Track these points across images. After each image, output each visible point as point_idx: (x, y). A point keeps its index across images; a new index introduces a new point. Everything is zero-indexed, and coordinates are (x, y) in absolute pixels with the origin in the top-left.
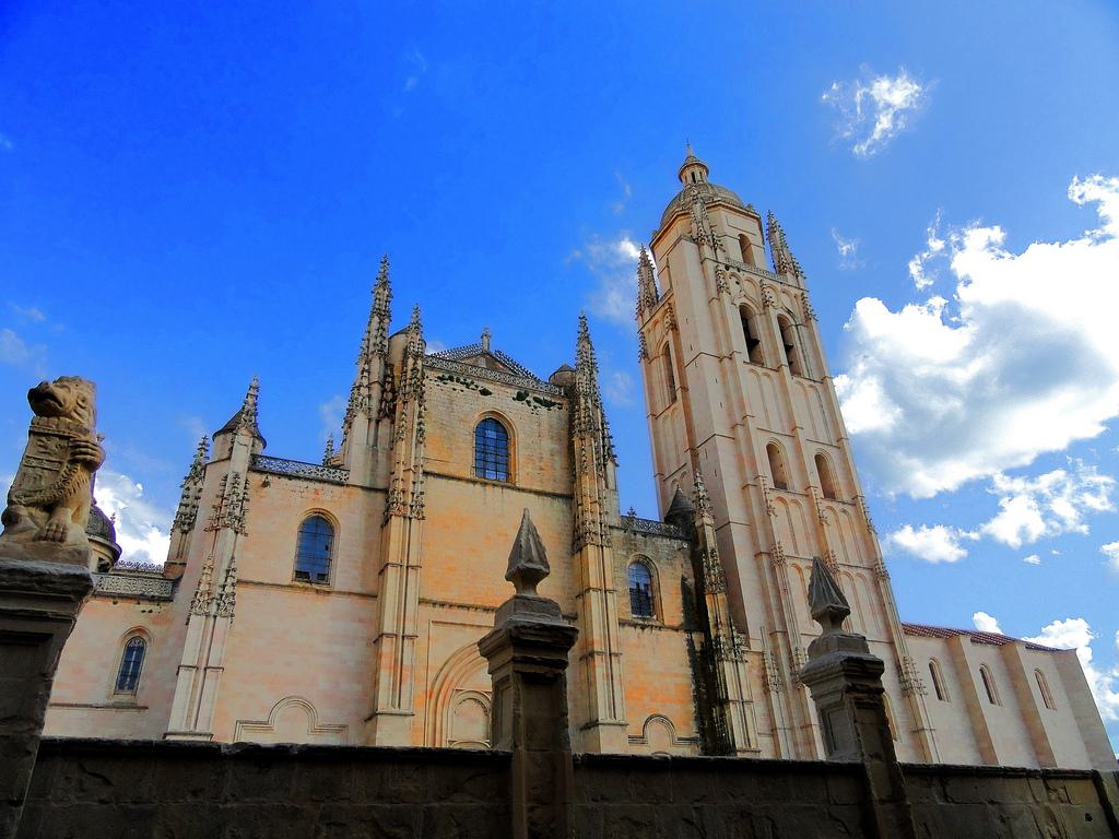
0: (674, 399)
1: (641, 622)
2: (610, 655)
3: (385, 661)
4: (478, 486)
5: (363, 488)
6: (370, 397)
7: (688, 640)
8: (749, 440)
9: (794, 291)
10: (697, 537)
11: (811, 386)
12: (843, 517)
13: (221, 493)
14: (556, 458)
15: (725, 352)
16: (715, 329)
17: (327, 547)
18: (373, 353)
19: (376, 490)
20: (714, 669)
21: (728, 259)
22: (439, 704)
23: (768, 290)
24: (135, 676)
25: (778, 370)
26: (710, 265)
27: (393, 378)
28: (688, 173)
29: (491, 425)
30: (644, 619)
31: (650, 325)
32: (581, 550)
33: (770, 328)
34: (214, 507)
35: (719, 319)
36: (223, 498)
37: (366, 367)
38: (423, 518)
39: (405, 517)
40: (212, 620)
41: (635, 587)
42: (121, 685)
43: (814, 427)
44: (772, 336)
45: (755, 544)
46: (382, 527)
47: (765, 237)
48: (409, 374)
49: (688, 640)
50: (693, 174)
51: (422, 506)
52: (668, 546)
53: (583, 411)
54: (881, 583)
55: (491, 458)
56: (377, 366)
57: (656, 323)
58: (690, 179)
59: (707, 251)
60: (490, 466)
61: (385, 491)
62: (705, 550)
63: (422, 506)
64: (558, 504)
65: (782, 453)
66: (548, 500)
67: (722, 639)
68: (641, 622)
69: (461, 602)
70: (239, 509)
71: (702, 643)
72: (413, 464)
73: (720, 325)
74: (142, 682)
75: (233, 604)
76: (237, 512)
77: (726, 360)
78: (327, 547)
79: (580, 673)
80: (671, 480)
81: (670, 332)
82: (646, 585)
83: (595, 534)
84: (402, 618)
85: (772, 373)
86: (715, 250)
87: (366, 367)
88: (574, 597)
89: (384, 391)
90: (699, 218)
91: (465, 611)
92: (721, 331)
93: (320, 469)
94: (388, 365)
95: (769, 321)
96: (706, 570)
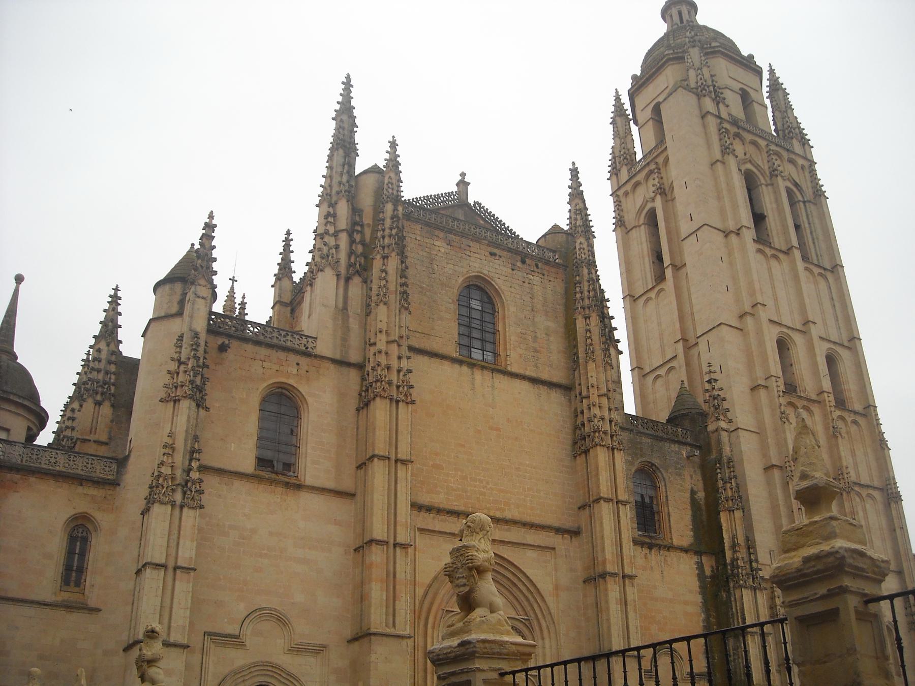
0: (660, 278)
1: (647, 540)
2: (624, 577)
3: (378, 573)
4: (465, 369)
5: (334, 361)
6: (337, 247)
7: (697, 563)
8: (759, 332)
9: (800, 162)
10: (709, 444)
11: (820, 274)
12: (854, 428)
13: (176, 356)
14: (552, 339)
15: (731, 225)
16: (719, 198)
17: (292, 432)
18: (338, 193)
19: (349, 365)
20: (729, 597)
21: (729, 114)
22: (430, 626)
23: (774, 157)
24: (81, 570)
25: (787, 252)
26: (712, 122)
27: (362, 226)
28: (674, 12)
29: (475, 294)
30: (650, 537)
31: (628, 187)
32: (586, 452)
33: (778, 201)
34: (169, 372)
35: (724, 186)
36: (180, 363)
37: (331, 210)
38: (413, 402)
39: (391, 400)
40: (177, 511)
41: (639, 499)
42: (66, 581)
43: (825, 323)
44: (780, 210)
45: (765, 455)
46: (358, 410)
47: (766, 95)
48: (388, 222)
49: (697, 563)
50: (680, 14)
51: (412, 387)
52: (676, 453)
53: (586, 284)
54: (893, 505)
55: (476, 334)
56: (343, 209)
57: (637, 184)
58: (676, 18)
59: (708, 104)
60: (477, 344)
61: (360, 367)
62: (719, 460)
63: (412, 387)
64: (556, 396)
65: (793, 352)
66: (543, 390)
67: (740, 563)
68: (647, 540)
69: (448, 507)
70: (199, 377)
71: (712, 567)
72: (397, 335)
73: (725, 192)
74: (89, 579)
75: (201, 492)
76: (198, 380)
77: (733, 237)
78: (292, 432)
79: (585, 596)
80: (653, 376)
81: (658, 198)
82: (651, 498)
83: (605, 433)
84: (393, 522)
85: (781, 256)
86: (718, 104)
87: (331, 210)
88: (576, 507)
89: (352, 242)
90: (697, 64)
91: (451, 519)
92: (726, 200)
93: (283, 333)
94: (356, 211)
95: (776, 192)
96: (720, 483)
